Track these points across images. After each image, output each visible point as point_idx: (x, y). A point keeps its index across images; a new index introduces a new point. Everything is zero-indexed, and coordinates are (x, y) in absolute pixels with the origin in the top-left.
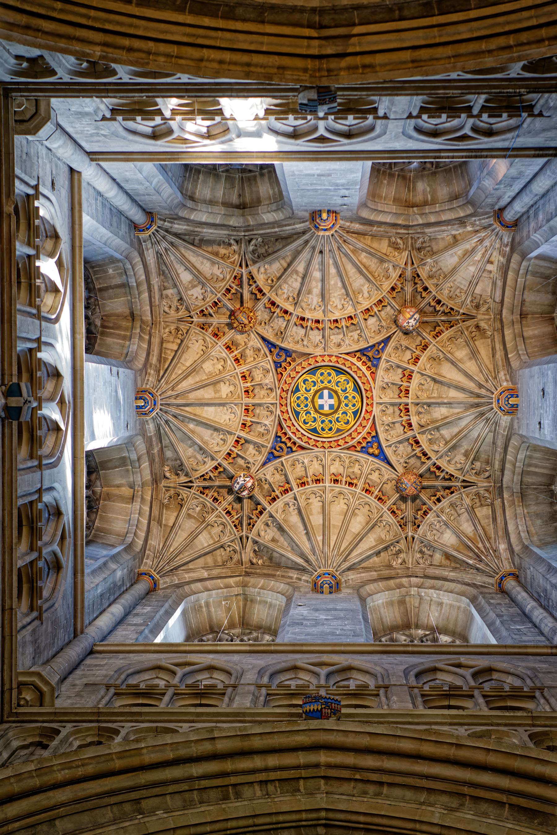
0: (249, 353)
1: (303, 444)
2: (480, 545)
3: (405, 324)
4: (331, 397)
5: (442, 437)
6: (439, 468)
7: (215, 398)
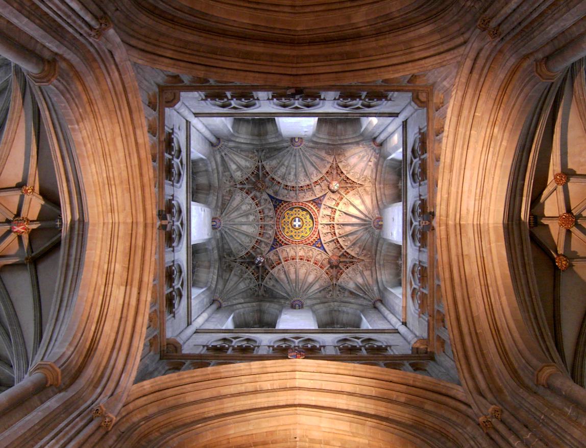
0: (262, 201)
2: (366, 288)
5: (349, 239)
6: (348, 253)
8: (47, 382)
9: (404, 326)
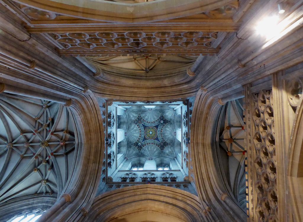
8: (66, 201)
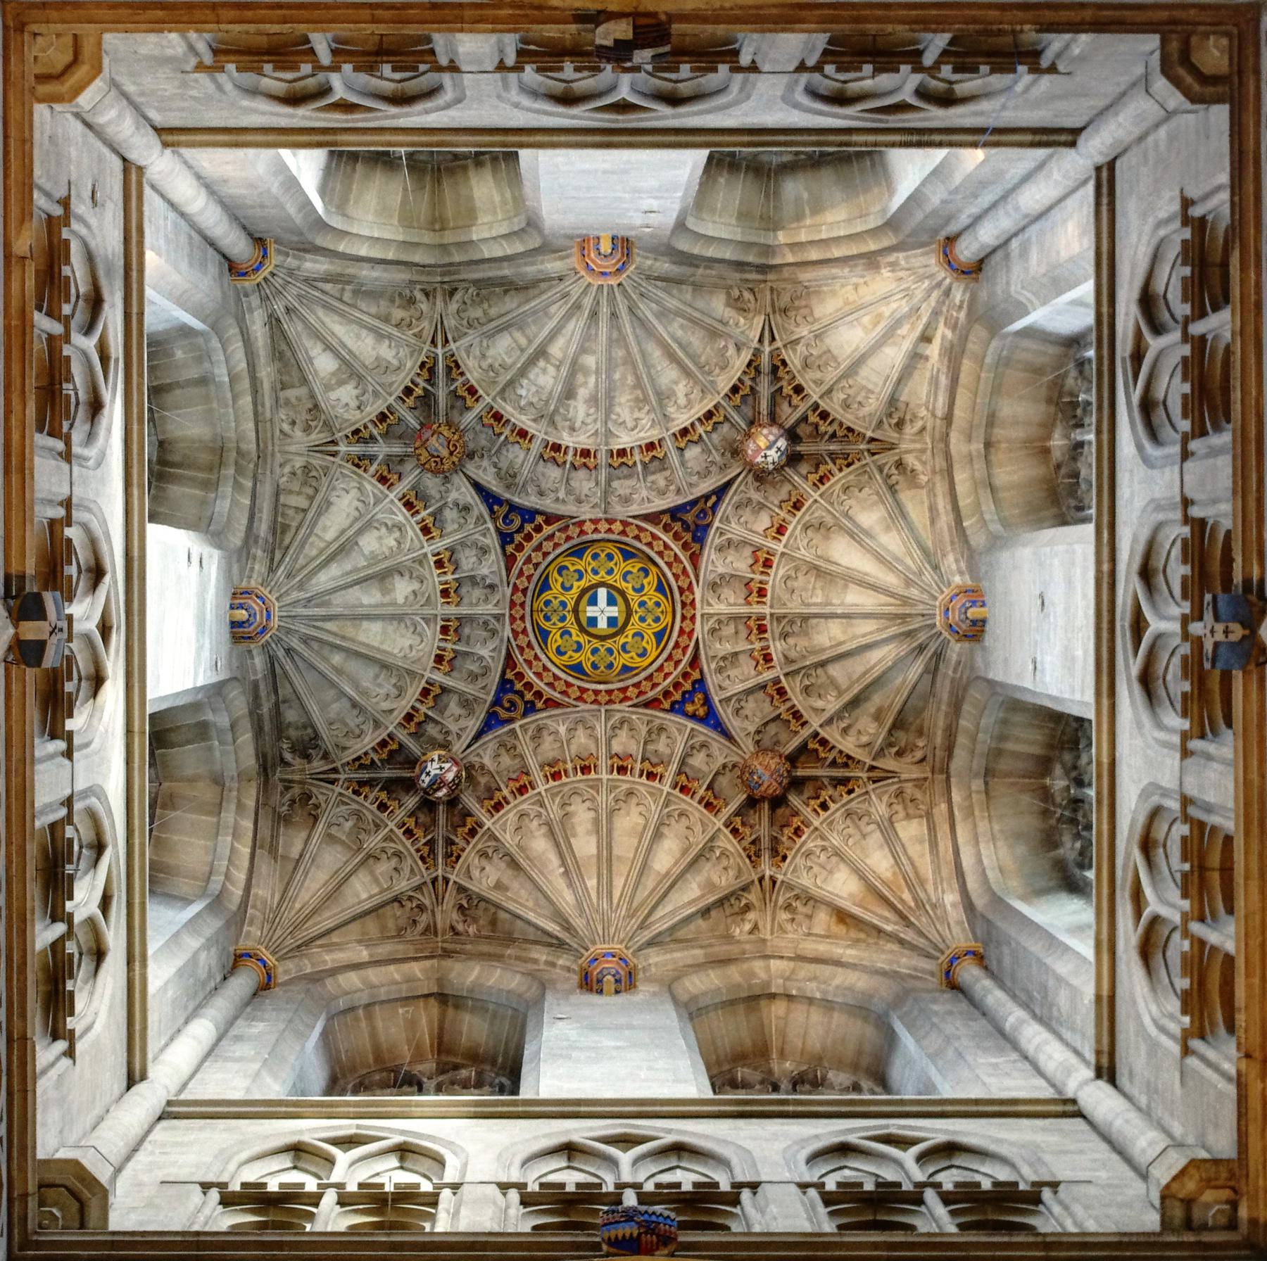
0: (450, 514)
1: (556, 695)
2: (907, 896)
3: (759, 459)
4: (611, 601)
7: (383, 605)
9: (1103, 1085)
